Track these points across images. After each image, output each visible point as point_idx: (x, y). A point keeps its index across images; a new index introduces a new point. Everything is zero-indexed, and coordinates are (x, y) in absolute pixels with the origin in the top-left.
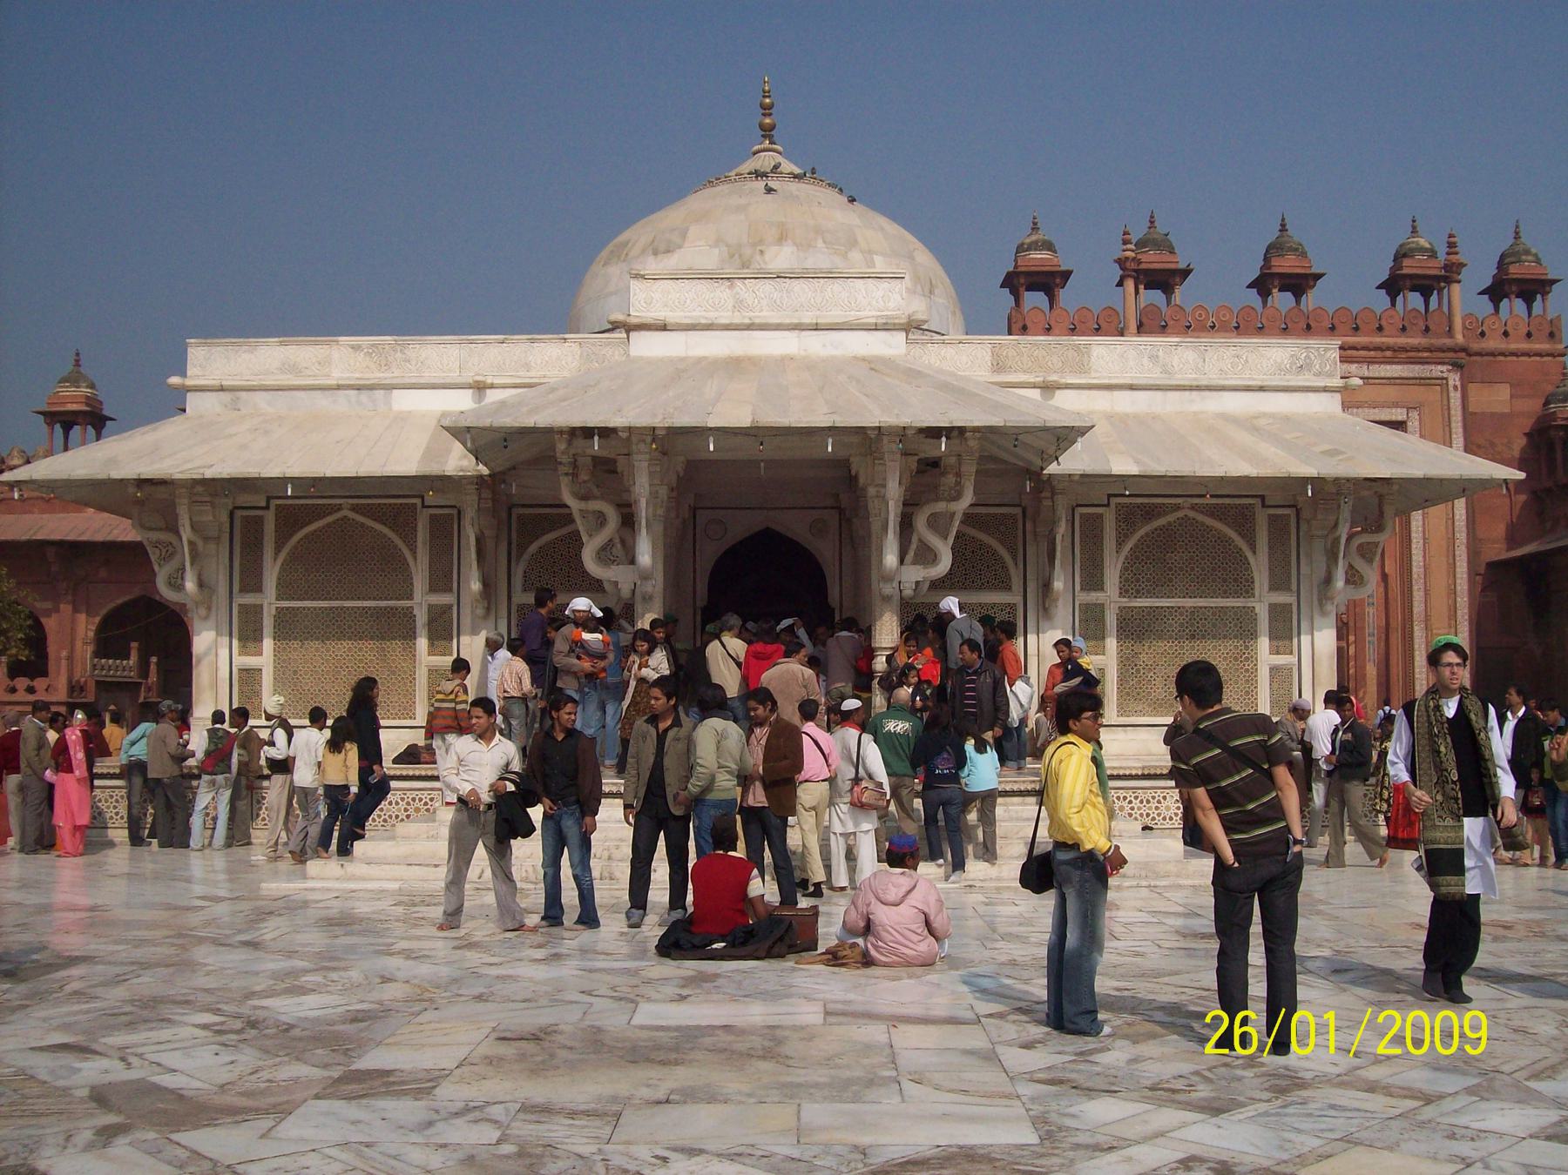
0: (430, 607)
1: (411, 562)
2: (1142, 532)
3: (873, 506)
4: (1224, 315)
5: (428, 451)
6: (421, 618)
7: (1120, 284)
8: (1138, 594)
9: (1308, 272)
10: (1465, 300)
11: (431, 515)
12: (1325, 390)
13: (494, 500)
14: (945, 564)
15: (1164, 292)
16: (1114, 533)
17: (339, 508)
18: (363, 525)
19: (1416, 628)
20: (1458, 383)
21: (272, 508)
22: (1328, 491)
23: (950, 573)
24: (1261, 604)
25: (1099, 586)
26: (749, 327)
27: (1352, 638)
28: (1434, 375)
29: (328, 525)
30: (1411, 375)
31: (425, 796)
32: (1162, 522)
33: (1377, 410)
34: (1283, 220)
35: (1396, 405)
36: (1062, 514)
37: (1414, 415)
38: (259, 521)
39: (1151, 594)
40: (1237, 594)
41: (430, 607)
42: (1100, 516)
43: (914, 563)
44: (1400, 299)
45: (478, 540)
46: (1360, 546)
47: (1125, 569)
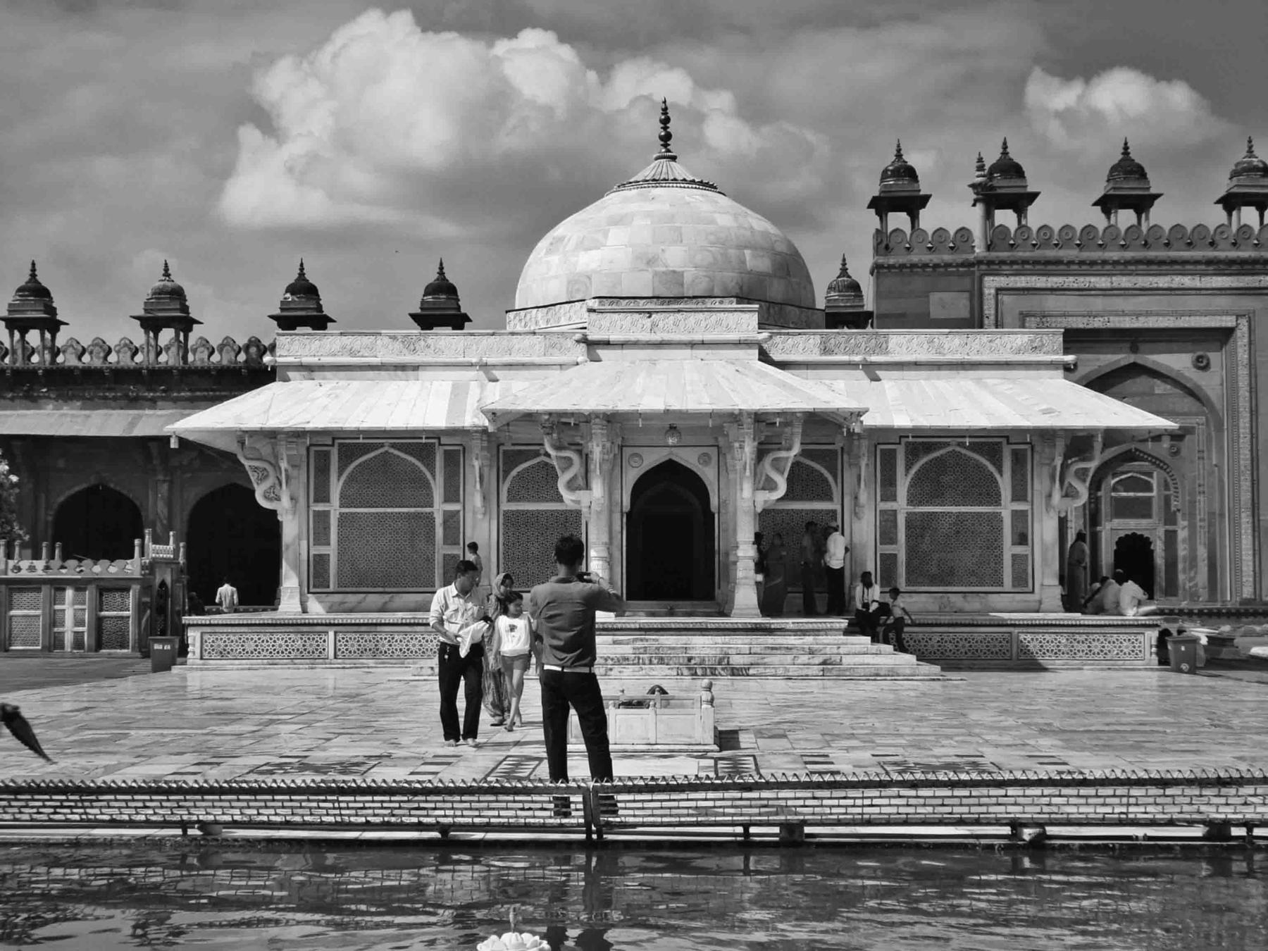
0: (445, 512)
1: (432, 481)
3: (737, 454)
4: (1067, 234)
5: (450, 411)
6: (439, 520)
7: (974, 205)
8: (920, 504)
9: (1146, 193)
11: (446, 451)
13: (489, 442)
14: (782, 489)
15: (1015, 211)
16: (903, 462)
17: (382, 445)
18: (398, 457)
19: (1243, 515)
21: (336, 445)
22: (1047, 435)
24: (1006, 509)
25: (893, 498)
27: (1182, 523)
29: (375, 457)
30: (1241, 285)
33: (1207, 318)
34: (1126, 144)
35: (1227, 313)
36: (864, 450)
37: (1244, 323)
40: (989, 504)
42: (894, 451)
43: (763, 489)
44: (1234, 213)
46: (1077, 472)
47: (911, 486)
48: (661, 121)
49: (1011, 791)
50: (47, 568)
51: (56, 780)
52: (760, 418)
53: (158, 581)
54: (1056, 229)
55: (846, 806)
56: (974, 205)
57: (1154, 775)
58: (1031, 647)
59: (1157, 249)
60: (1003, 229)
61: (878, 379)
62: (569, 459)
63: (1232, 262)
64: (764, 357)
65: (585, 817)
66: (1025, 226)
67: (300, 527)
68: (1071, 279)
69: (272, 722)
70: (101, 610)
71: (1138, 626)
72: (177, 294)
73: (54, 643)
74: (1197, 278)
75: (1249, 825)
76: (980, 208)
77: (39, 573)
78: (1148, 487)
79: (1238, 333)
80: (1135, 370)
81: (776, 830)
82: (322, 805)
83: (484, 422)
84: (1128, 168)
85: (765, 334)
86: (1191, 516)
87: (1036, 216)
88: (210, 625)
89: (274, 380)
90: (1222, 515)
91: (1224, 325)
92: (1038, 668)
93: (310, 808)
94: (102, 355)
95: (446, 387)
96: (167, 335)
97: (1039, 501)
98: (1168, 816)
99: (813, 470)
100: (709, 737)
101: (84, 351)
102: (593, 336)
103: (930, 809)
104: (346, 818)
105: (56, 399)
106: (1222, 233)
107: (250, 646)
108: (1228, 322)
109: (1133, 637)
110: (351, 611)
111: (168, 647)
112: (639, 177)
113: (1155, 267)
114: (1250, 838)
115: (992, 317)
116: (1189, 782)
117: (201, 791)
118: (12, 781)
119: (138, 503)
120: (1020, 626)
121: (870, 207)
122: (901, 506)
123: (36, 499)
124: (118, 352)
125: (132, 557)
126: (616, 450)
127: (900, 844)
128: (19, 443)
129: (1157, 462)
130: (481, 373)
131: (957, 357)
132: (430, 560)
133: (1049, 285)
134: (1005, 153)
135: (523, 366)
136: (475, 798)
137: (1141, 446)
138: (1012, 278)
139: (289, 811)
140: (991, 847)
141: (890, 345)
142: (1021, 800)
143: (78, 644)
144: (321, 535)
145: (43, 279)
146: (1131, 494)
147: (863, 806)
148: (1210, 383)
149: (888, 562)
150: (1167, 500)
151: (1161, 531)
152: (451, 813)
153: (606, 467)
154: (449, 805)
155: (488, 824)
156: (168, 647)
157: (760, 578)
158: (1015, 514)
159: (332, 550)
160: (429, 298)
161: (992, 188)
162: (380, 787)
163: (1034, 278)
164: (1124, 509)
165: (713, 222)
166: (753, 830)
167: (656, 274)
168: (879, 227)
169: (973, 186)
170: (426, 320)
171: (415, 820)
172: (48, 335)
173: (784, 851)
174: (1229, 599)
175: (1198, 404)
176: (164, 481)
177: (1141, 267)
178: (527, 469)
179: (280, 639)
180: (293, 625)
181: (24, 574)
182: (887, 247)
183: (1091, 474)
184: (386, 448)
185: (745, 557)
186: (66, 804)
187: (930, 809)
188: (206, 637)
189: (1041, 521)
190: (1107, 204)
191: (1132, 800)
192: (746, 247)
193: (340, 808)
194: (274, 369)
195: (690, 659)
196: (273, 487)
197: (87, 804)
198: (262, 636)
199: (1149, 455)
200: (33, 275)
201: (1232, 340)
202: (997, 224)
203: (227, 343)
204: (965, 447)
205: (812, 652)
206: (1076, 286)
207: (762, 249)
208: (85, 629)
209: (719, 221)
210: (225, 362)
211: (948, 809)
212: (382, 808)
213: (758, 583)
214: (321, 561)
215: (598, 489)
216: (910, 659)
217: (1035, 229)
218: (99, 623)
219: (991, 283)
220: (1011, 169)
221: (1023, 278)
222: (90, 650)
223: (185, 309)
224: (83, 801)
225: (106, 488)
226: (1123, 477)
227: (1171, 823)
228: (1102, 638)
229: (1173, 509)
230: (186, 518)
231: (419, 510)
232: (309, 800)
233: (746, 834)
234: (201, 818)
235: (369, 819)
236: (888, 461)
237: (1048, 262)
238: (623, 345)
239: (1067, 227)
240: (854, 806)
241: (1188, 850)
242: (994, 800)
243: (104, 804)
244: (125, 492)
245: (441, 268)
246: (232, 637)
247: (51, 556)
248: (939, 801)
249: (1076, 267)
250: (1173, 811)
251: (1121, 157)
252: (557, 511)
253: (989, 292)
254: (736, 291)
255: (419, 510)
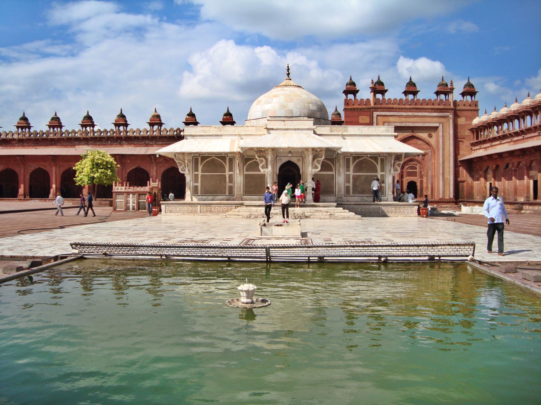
0: (229, 174)
1: (225, 166)
2: (357, 161)
3: (307, 159)
6: (227, 176)
7: (371, 93)
8: (356, 172)
10: (456, 96)
11: (229, 158)
12: (391, 136)
20: (452, 117)
22: (390, 154)
23: (321, 169)
24: (379, 174)
25: (349, 171)
26: (287, 129)
28: (446, 115)
30: (440, 115)
31: (230, 207)
32: (361, 159)
33: (432, 124)
35: (436, 122)
36: (341, 158)
37: (441, 125)
38: (197, 159)
39: (359, 172)
41: (229, 174)
43: (314, 168)
44: (439, 96)
45: (238, 163)
47: (354, 167)
48: (287, 70)
49: (379, 248)
50: (125, 189)
51: (128, 244)
52: (313, 149)
53: (154, 193)
54: (392, 100)
55: (335, 252)
56: (371, 93)
57: (416, 244)
58: (385, 211)
59: (419, 105)
60: (379, 99)
61: (345, 139)
62: (262, 160)
63: (438, 109)
64: (315, 133)
65: (266, 255)
66: (384, 98)
67: (191, 178)
68: (396, 113)
69: (184, 229)
70: (139, 200)
71: (413, 205)
72: (158, 116)
73: (127, 208)
74: (429, 113)
75: (439, 256)
76: (372, 94)
77: (123, 190)
78: (416, 169)
79: (440, 128)
80: (413, 137)
81: (317, 258)
82: (197, 251)
83: (239, 150)
84: (411, 84)
85: (315, 127)
86: (427, 176)
87: (387, 96)
88: (167, 204)
89: (183, 139)
90: (435, 176)
91: (436, 126)
92: (386, 216)
93: (194, 252)
94: (139, 133)
95: (230, 141)
96: (156, 127)
97: (387, 172)
98: (419, 254)
99: (328, 163)
100: (299, 234)
101: (134, 132)
102: (268, 127)
103: (357, 253)
104: (203, 254)
105: (127, 144)
106: (436, 101)
107: (178, 209)
108: (437, 125)
109: (411, 208)
110: (204, 200)
111: (156, 210)
112: (281, 84)
113: (418, 110)
114: (440, 260)
115: (376, 123)
116: (425, 246)
117: (165, 247)
118: (117, 243)
119: (148, 172)
120: (382, 205)
121: (343, 93)
122: (351, 173)
123: (122, 170)
124: (143, 132)
125: (147, 186)
126: (275, 158)
127: (349, 262)
128: (117, 156)
129: (419, 162)
130: (239, 137)
131: (366, 133)
132: (225, 187)
133: (391, 114)
134: (379, 79)
135: (250, 135)
136: (237, 249)
137: (414, 158)
138: (381, 112)
139: (188, 252)
140: (373, 263)
141: (349, 130)
142: (381, 250)
143: (133, 209)
144: (196, 181)
145: (124, 113)
146: (412, 170)
147: (340, 252)
148: (432, 141)
149: (347, 188)
150: (421, 172)
151: (419, 180)
152: (231, 253)
153: (272, 162)
154: (230, 251)
155: (241, 256)
156: (156, 210)
157: (313, 192)
158: (381, 175)
159: (199, 185)
160: (225, 117)
161: (376, 88)
162: (212, 246)
163: (387, 112)
164: (410, 174)
165: (301, 97)
166: (310, 258)
167: (286, 110)
168: (345, 98)
169: (371, 88)
170: (224, 123)
171: (221, 255)
172: (125, 128)
173: (319, 264)
174: (436, 198)
175: (429, 146)
176: (155, 166)
177: (414, 110)
178: (251, 163)
179: (186, 208)
180: (189, 204)
181: (119, 190)
182: (348, 104)
183: (401, 165)
184: (213, 157)
185: (309, 187)
186: (131, 249)
187: (357, 253)
188: (166, 207)
189: (388, 177)
190: (406, 93)
191: (410, 250)
192: (311, 103)
193: (202, 252)
194: (184, 136)
195: (294, 214)
196: (183, 167)
197: (136, 250)
198: (181, 207)
199: (416, 160)
200: (121, 112)
201: (438, 130)
202: (377, 98)
203: (171, 129)
204: (368, 157)
205: (327, 212)
206: (397, 115)
207: (315, 104)
208: (135, 205)
209: (303, 97)
210: (171, 135)
211: (362, 253)
212: (213, 252)
213: (313, 194)
214: (196, 188)
215: (270, 168)
216: (353, 214)
217: (387, 100)
218: (139, 203)
219: (375, 114)
220: (380, 83)
221: (384, 112)
222: (136, 210)
223: (160, 120)
224: (135, 249)
225: (140, 168)
226: (410, 166)
227: (420, 256)
228: (403, 208)
229: (422, 174)
230: (161, 175)
231: (222, 174)
232: (193, 250)
233: (309, 259)
234: (166, 254)
235: (210, 255)
236: (348, 161)
237: (390, 108)
238: (277, 129)
239: (395, 99)
240: (337, 252)
241: (424, 263)
242: (374, 250)
243: (141, 250)
244: (145, 169)
245: (228, 109)
246: (173, 207)
247: (126, 186)
248: (360, 251)
249: (397, 110)
250: (420, 253)
251: (409, 81)
252: (259, 174)
253: (375, 116)
254: (307, 115)
255: (222, 174)
